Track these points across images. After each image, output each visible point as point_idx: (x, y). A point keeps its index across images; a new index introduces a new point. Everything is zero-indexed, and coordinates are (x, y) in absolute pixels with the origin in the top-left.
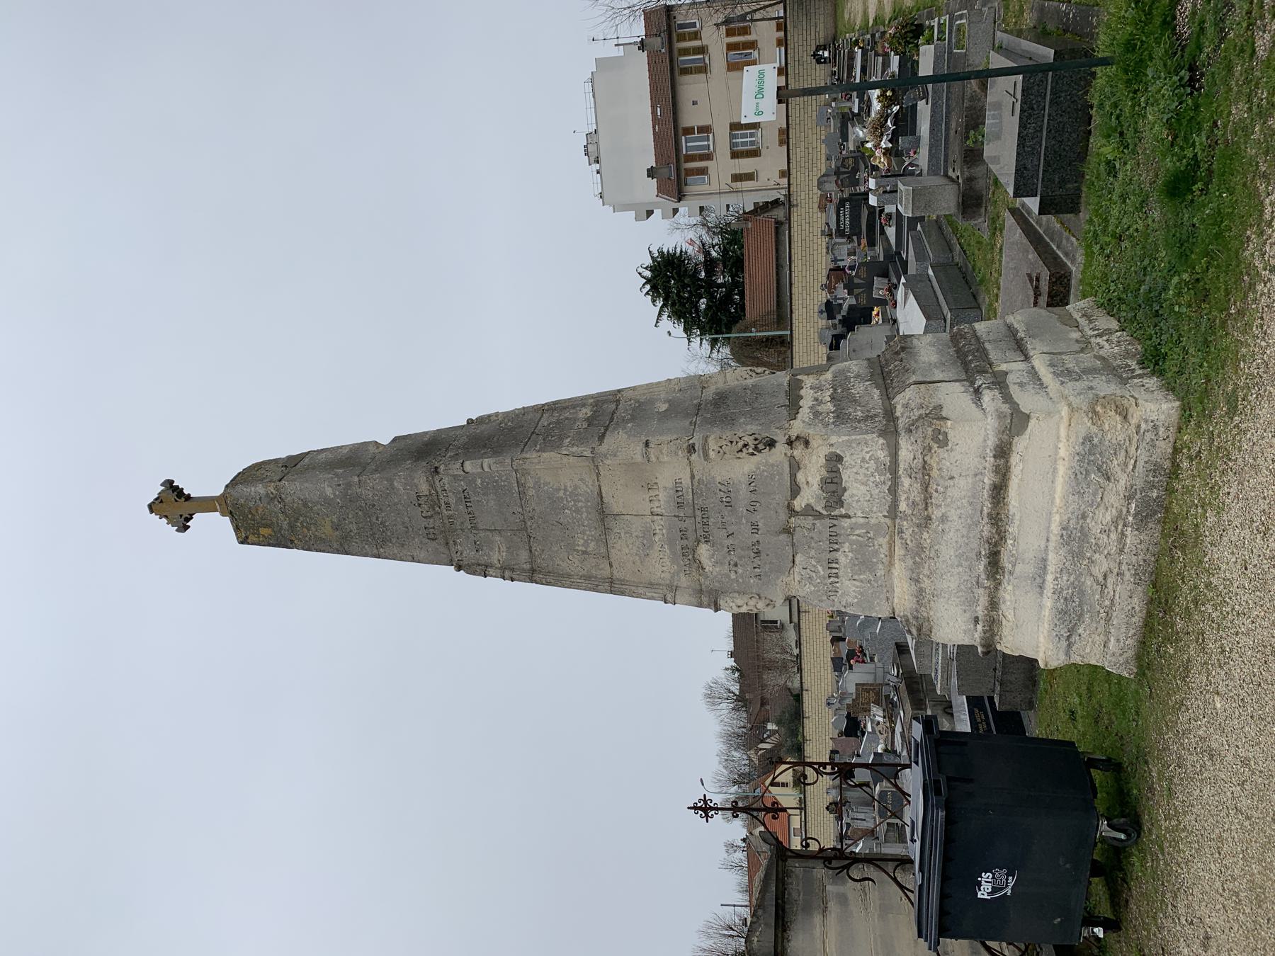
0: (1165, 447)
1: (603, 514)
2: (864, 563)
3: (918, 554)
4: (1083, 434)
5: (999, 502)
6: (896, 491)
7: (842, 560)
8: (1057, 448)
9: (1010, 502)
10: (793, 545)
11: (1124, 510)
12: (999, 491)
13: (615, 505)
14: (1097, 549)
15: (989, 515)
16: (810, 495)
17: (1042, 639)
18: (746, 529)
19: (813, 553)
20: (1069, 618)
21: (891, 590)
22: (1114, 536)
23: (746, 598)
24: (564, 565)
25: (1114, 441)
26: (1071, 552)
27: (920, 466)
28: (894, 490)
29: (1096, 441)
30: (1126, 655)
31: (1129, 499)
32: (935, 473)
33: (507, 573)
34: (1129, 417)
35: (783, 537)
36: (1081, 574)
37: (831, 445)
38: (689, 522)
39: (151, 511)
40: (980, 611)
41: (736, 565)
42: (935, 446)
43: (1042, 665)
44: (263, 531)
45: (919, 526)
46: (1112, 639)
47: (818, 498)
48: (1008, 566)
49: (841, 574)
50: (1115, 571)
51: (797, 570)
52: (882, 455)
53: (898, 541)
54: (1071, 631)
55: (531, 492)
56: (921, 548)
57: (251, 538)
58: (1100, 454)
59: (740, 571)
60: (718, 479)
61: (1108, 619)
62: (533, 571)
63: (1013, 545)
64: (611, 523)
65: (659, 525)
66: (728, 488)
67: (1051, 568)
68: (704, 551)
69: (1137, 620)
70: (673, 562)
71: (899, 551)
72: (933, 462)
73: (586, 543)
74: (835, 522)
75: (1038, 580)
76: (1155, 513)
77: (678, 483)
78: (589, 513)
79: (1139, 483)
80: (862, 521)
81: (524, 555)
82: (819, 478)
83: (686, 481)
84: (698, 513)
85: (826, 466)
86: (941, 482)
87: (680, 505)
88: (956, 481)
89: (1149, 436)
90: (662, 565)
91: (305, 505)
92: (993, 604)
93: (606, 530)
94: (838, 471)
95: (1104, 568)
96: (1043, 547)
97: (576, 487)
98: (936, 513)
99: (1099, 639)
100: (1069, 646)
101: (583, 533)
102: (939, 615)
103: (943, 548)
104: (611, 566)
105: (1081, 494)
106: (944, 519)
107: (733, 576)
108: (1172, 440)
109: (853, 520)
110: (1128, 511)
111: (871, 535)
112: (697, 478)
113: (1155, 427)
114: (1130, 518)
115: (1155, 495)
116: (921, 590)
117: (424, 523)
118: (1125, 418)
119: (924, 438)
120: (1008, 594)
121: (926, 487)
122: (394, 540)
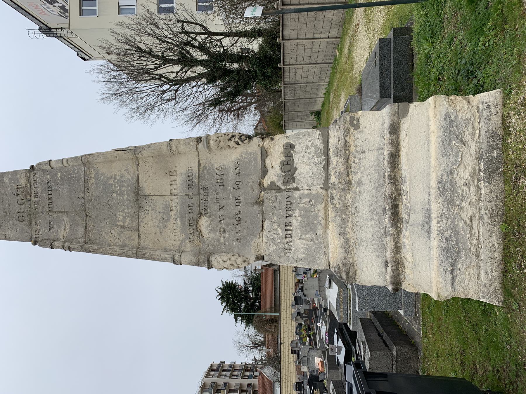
0: (497, 120)
1: (138, 196)
2: (309, 225)
3: (344, 211)
4: (444, 112)
5: (395, 167)
6: (328, 168)
7: (295, 223)
8: (428, 126)
9: (401, 197)
10: (262, 213)
11: (477, 168)
12: (394, 158)
13: (147, 188)
14: (463, 198)
15: (389, 176)
16: (274, 175)
17: (433, 275)
18: (232, 202)
19: (275, 219)
20: (451, 255)
21: (327, 247)
22: (473, 188)
23: (229, 256)
24: (107, 237)
25: (464, 118)
26: (446, 200)
27: (343, 144)
28: (326, 168)
29: (453, 118)
30: (494, 285)
31: (479, 159)
32: (352, 149)
33: (66, 245)
34: (471, 102)
35: (256, 207)
36: (455, 218)
37: (287, 137)
38: (195, 199)
40: (389, 255)
41: (224, 231)
42: (352, 129)
43: (434, 297)
45: (343, 190)
46: (482, 272)
48: (405, 216)
49: (293, 234)
50: (477, 215)
51: (265, 233)
52: (319, 142)
53: (330, 207)
54: (454, 265)
55: (92, 181)
56: (345, 206)
58: (457, 127)
59: (227, 236)
60: (216, 166)
61: (478, 255)
62: (86, 242)
63: (407, 199)
64: (142, 202)
65: (175, 203)
66: (222, 172)
67: (434, 215)
68: (204, 222)
69: (497, 255)
70: (182, 231)
71: (331, 214)
72: (351, 141)
74: (290, 194)
75: (426, 227)
76: (498, 168)
79: (484, 147)
80: (307, 192)
81: (81, 231)
82: (279, 162)
83: (195, 169)
84: (201, 191)
85: (284, 153)
86: (357, 155)
87: (190, 187)
88: (366, 154)
89: (485, 113)
90: (175, 234)
92: (397, 249)
93: (139, 208)
94: (291, 156)
95: (470, 213)
96: (427, 200)
98: (354, 179)
99: (473, 272)
100: (453, 279)
101: (123, 211)
102: (361, 260)
103: (360, 205)
104: (139, 237)
105: (447, 156)
106: (360, 183)
107: (222, 240)
108: (500, 114)
109: (301, 192)
110: (480, 169)
111: (313, 202)
112: (202, 165)
113: (489, 107)
114: (482, 174)
115: (495, 155)
116: (347, 240)
117: (17, 208)
118: (469, 102)
119: (345, 123)
120: (407, 239)
121: (347, 159)
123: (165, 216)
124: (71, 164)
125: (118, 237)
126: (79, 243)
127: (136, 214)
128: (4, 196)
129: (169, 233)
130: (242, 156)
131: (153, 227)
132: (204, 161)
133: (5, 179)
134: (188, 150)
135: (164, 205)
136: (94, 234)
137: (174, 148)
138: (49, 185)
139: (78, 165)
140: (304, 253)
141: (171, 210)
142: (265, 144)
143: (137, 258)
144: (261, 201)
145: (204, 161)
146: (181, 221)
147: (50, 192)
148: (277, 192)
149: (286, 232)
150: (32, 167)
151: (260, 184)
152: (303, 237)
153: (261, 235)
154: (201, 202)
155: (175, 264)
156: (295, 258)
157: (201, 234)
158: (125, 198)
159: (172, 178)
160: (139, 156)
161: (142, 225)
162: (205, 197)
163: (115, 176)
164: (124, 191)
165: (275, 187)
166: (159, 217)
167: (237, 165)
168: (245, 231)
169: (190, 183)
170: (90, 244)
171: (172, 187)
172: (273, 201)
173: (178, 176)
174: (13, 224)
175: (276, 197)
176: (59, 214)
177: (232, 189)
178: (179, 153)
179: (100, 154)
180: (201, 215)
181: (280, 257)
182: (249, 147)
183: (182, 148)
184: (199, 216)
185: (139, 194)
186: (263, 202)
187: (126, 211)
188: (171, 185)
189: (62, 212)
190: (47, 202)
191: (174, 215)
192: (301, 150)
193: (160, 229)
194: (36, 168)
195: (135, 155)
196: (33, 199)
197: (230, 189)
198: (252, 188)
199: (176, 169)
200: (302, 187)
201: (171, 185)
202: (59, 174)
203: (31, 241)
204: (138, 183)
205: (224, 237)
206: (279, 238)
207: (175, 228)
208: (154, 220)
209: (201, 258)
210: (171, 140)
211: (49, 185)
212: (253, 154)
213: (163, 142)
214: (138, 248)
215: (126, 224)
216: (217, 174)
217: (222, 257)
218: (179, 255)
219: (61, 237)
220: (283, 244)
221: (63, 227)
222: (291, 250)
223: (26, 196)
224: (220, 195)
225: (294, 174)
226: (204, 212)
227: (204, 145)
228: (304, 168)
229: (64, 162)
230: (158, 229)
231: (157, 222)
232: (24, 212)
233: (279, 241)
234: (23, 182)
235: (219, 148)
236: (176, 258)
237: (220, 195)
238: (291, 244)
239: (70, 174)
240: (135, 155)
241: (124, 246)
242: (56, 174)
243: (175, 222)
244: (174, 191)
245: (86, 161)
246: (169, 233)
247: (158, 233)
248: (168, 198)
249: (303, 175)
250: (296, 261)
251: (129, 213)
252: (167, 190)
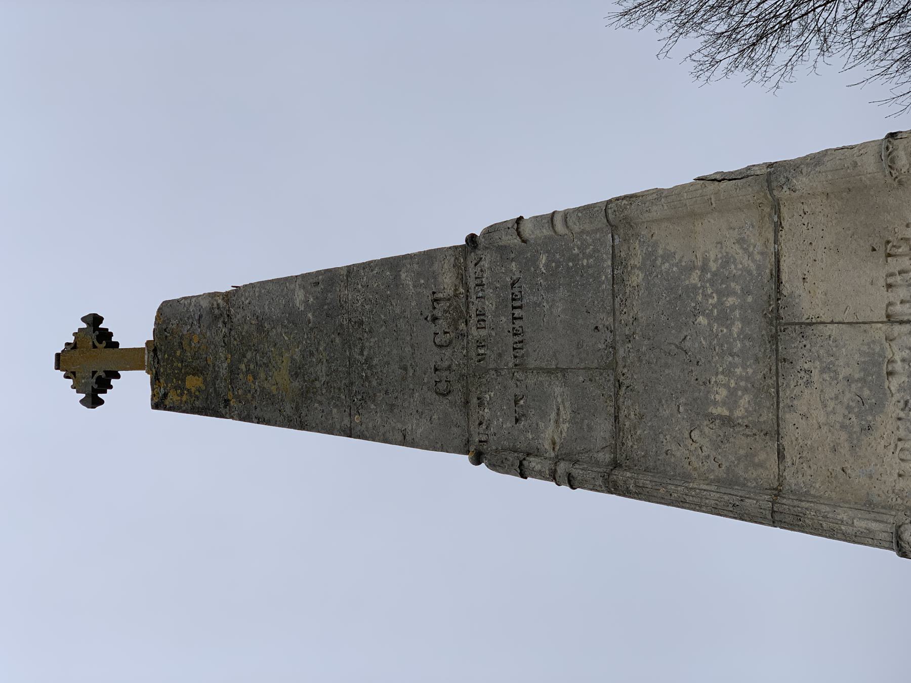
1: (778, 324)
13: (808, 298)
24: (679, 453)
33: (562, 467)
39: (58, 367)
44: (193, 382)
55: (637, 278)
57: (173, 397)
62: (616, 465)
73: (732, 401)
78: (745, 321)
81: (602, 429)
91: (260, 328)
97: (727, 261)
101: (728, 372)
104: (781, 456)
122: (380, 396)
123: (866, 393)
124: (576, 229)
125: (713, 454)
126: (597, 463)
127: (770, 382)
128: (402, 323)
129: (880, 449)
131: (825, 429)
133: (403, 276)
135: (862, 353)
136: (639, 439)
138: (516, 291)
139: (597, 230)
141: (890, 374)
143: (774, 524)
147: (517, 312)
150: (472, 239)
158: (735, 330)
160: (785, 193)
161: (790, 418)
163: (706, 260)
164: (733, 308)
166: (848, 395)
170: (629, 469)
171: (891, 296)
174: (423, 401)
176: (543, 378)
179: (658, 194)
185: (778, 318)
187: (738, 371)
188: (889, 286)
189: (549, 372)
190: (511, 340)
191: (901, 389)
194: (482, 242)
196: (474, 331)
201: (889, 286)
202: (543, 259)
203: (467, 453)
204: (779, 282)
207: (902, 433)
210: (892, 135)
211: (516, 291)
213: (865, 145)
214: (777, 492)
215: (738, 413)
219: (547, 445)
221: (553, 416)
223: (455, 323)
229: (558, 221)
230: (844, 436)
231: (841, 410)
232: (449, 368)
234: (447, 281)
239: (574, 258)
241: (730, 482)
242: (534, 260)
243: (902, 415)
244: (898, 308)
245: (617, 218)
246: (880, 449)
247: (845, 450)
248: (879, 332)
251: (747, 379)
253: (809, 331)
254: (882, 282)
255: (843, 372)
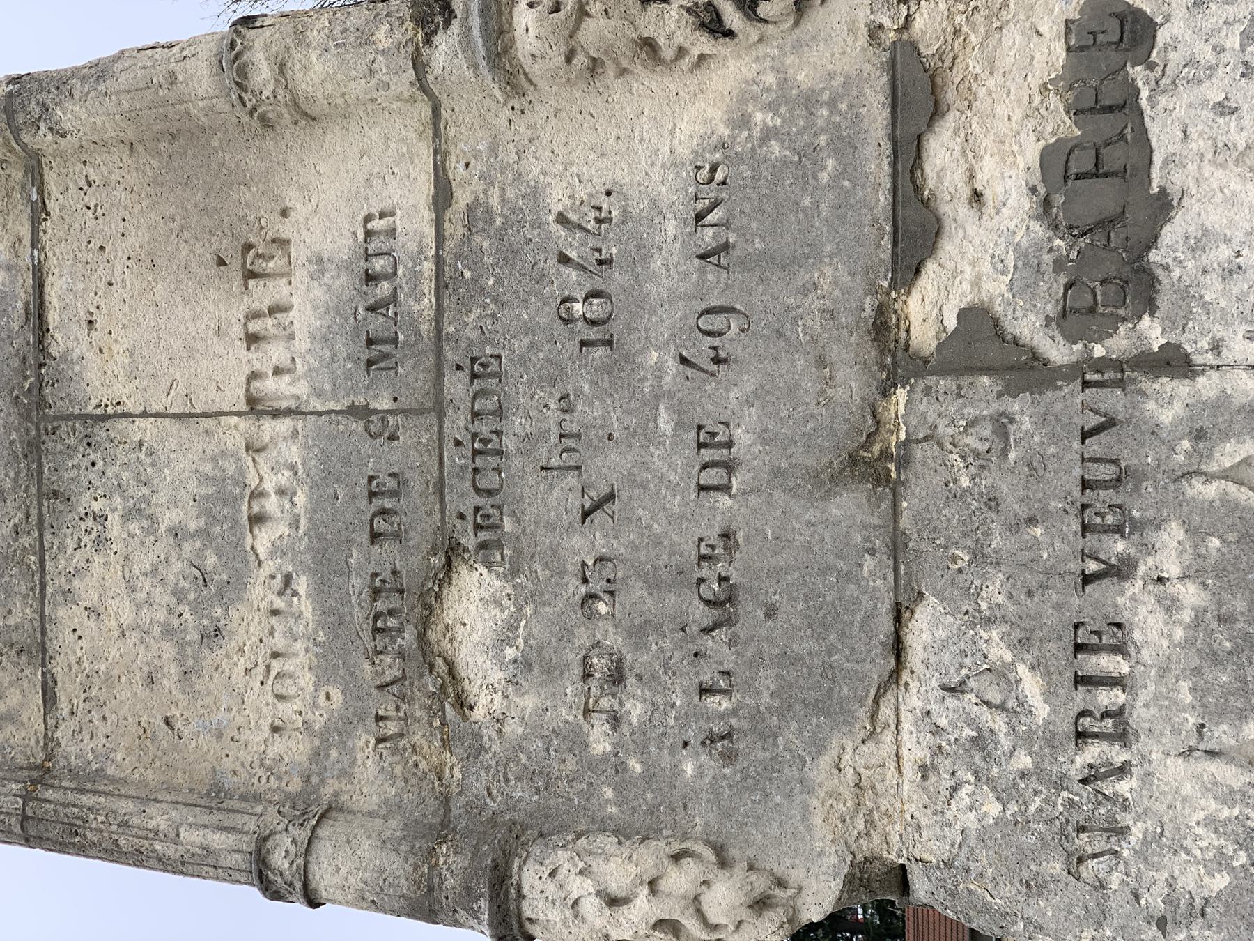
7: (1153, 630)
10: (897, 547)
13: (100, 368)
16: (991, 251)
18: (671, 460)
19: (994, 592)
23: (649, 857)
35: (850, 507)
41: (617, 677)
47: (1028, 267)
49: (1141, 715)
51: (915, 696)
59: (635, 710)
60: (558, 198)
64: (71, 468)
65: (281, 466)
66: (602, 239)
68: (475, 607)
70: (325, 671)
74: (1113, 401)
77: (374, 236)
82: (1031, 153)
83: (415, 223)
87: (377, 353)
90: (273, 689)
94: (1126, 106)
104: (49, 698)
107: (600, 741)
109: (1207, 385)
112: (462, 198)
123: (211, 560)
127: (27, 541)
129: (238, 677)
130: (744, 122)
131: (133, 637)
132: (477, 166)
134: (358, 88)
135: (204, 479)
137: (262, 74)
140: (1221, 862)
141: (257, 520)
142: (918, 23)
143: (28, 841)
144: (885, 455)
145: (477, 166)
146: (320, 591)
148: (1011, 391)
149: (1080, 699)
151: (884, 328)
152: (1221, 734)
153: (886, 712)
154: (456, 459)
155: (276, 896)
156: (1155, 900)
157: (452, 692)
159: (261, 294)
160: (43, 140)
161: (66, 616)
162: (484, 428)
165: (991, 352)
166: (176, 566)
167: (713, 184)
168: (768, 680)
169: (377, 324)
172: (980, 461)
173: (301, 275)
175: (1002, 424)
177: (673, 365)
178: (305, 115)
180: (452, 553)
181: (1035, 887)
182: (797, 47)
183: (316, 72)
184: (437, 561)
185: (42, 404)
186: (904, 462)
191: (276, 550)
192: (1207, 55)
193: (181, 646)
195: (16, 131)
197: (660, 368)
198: (821, 361)
199: (286, 229)
200: (1216, 347)
201: (253, 339)
204: (42, 329)
205: (615, 721)
206: (1028, 740)
207: (279, 642)
208: (145, 585)
209: (453, 864)
212: (832, 105)
213: (193, 42)
214: (41, 773)
216: (564, 259)
217: (597, 864)
218: (302, 835)
220: (1060, 784)
222: (1123, 832)
224: (588, 412)
225: (1152, 242)
226: (475, 534)
227: (467, 41)
228: (1231, 201)
230: (169, 650)
231: (163, 597)
233: (1024, 761)
235: (580, 61)
236: (279, 860)
237: (588, 412)
238: (1123, 787)
240: (16, 131)
243: (279, 603)
244: (270, 385)
246: (238, 677)
248: (235, 432)
249: (1225, 252)
250: (1162, 923)
252: (223, 374)
253: (100, 434)
254: (237, 331)
255: (169, 518)
